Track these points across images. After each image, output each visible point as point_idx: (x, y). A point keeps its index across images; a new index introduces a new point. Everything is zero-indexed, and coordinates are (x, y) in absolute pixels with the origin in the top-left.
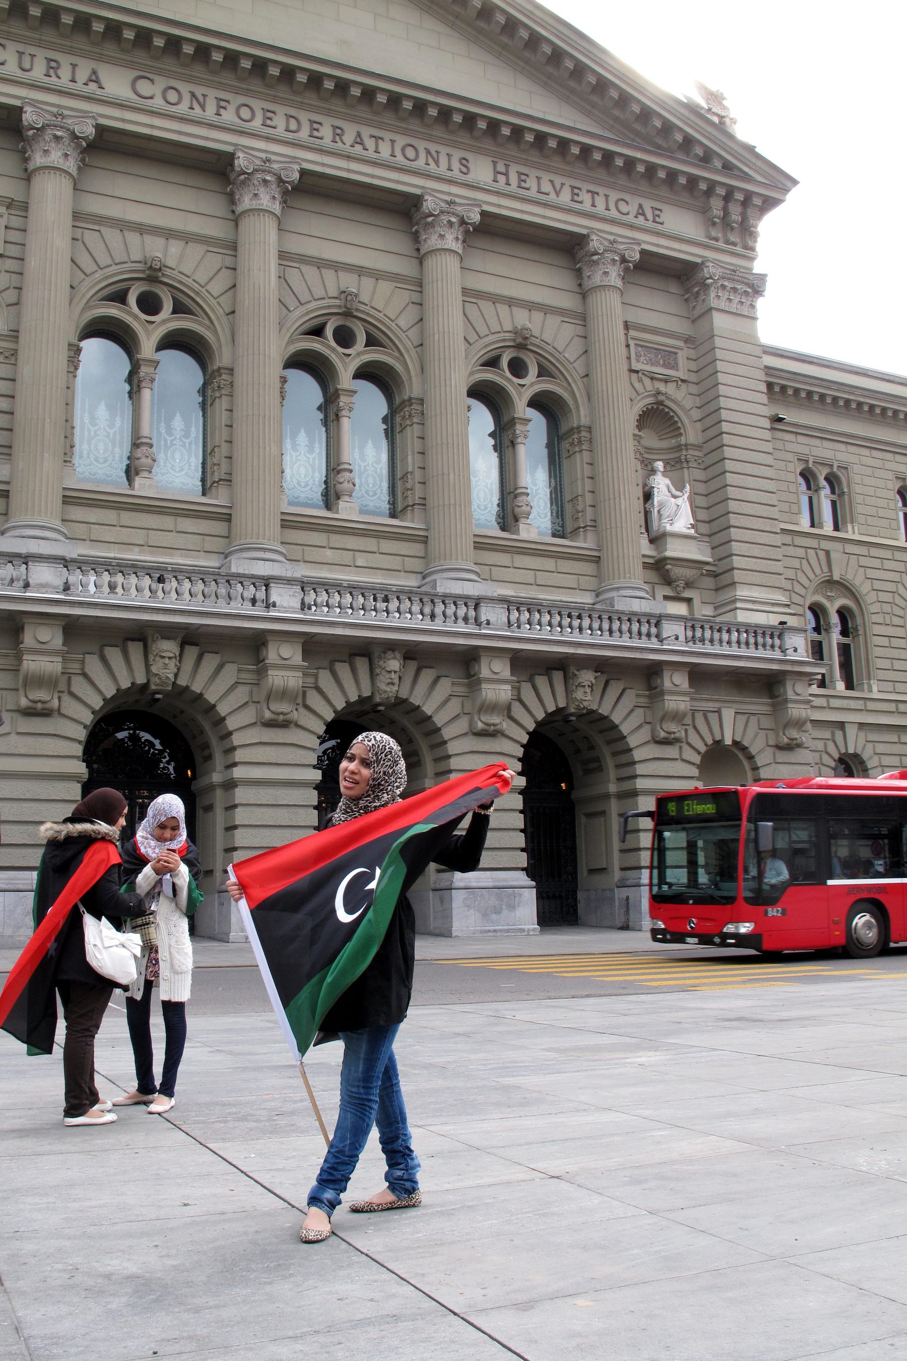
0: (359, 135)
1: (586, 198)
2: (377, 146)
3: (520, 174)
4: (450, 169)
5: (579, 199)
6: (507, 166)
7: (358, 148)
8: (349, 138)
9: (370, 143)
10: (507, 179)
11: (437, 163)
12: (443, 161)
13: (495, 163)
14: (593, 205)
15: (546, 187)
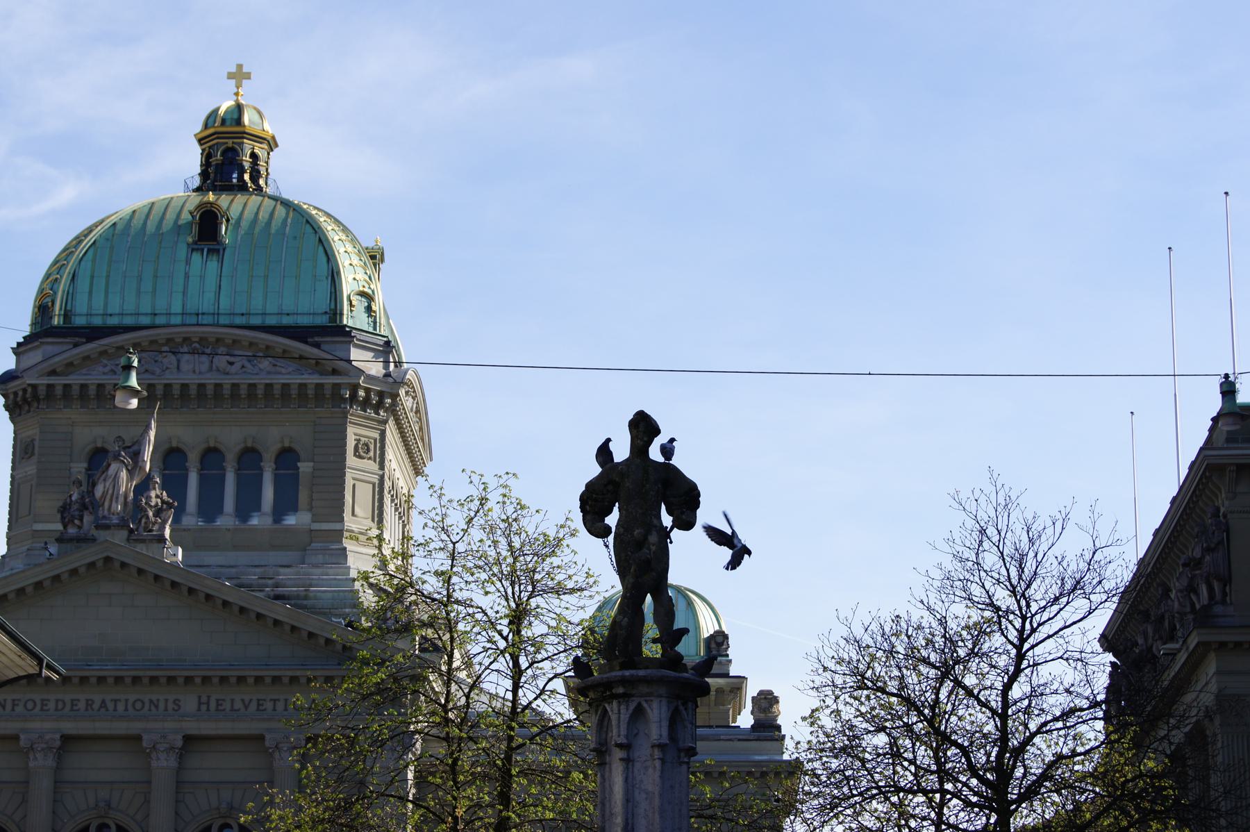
0: (103, 702)
1: (269, 705)
2: (115, 706)
3: (217, 700)
4: (166, 710)
5: (264, 707)
6: (209, 697)
7: (103, 710)
8: (96, 706)
9: (110, 706)
10: (208, 706)
11: (157, 707)
12: (162, 706)
13: (200, 697)
14: (274, 709)
15: (238, 705)
